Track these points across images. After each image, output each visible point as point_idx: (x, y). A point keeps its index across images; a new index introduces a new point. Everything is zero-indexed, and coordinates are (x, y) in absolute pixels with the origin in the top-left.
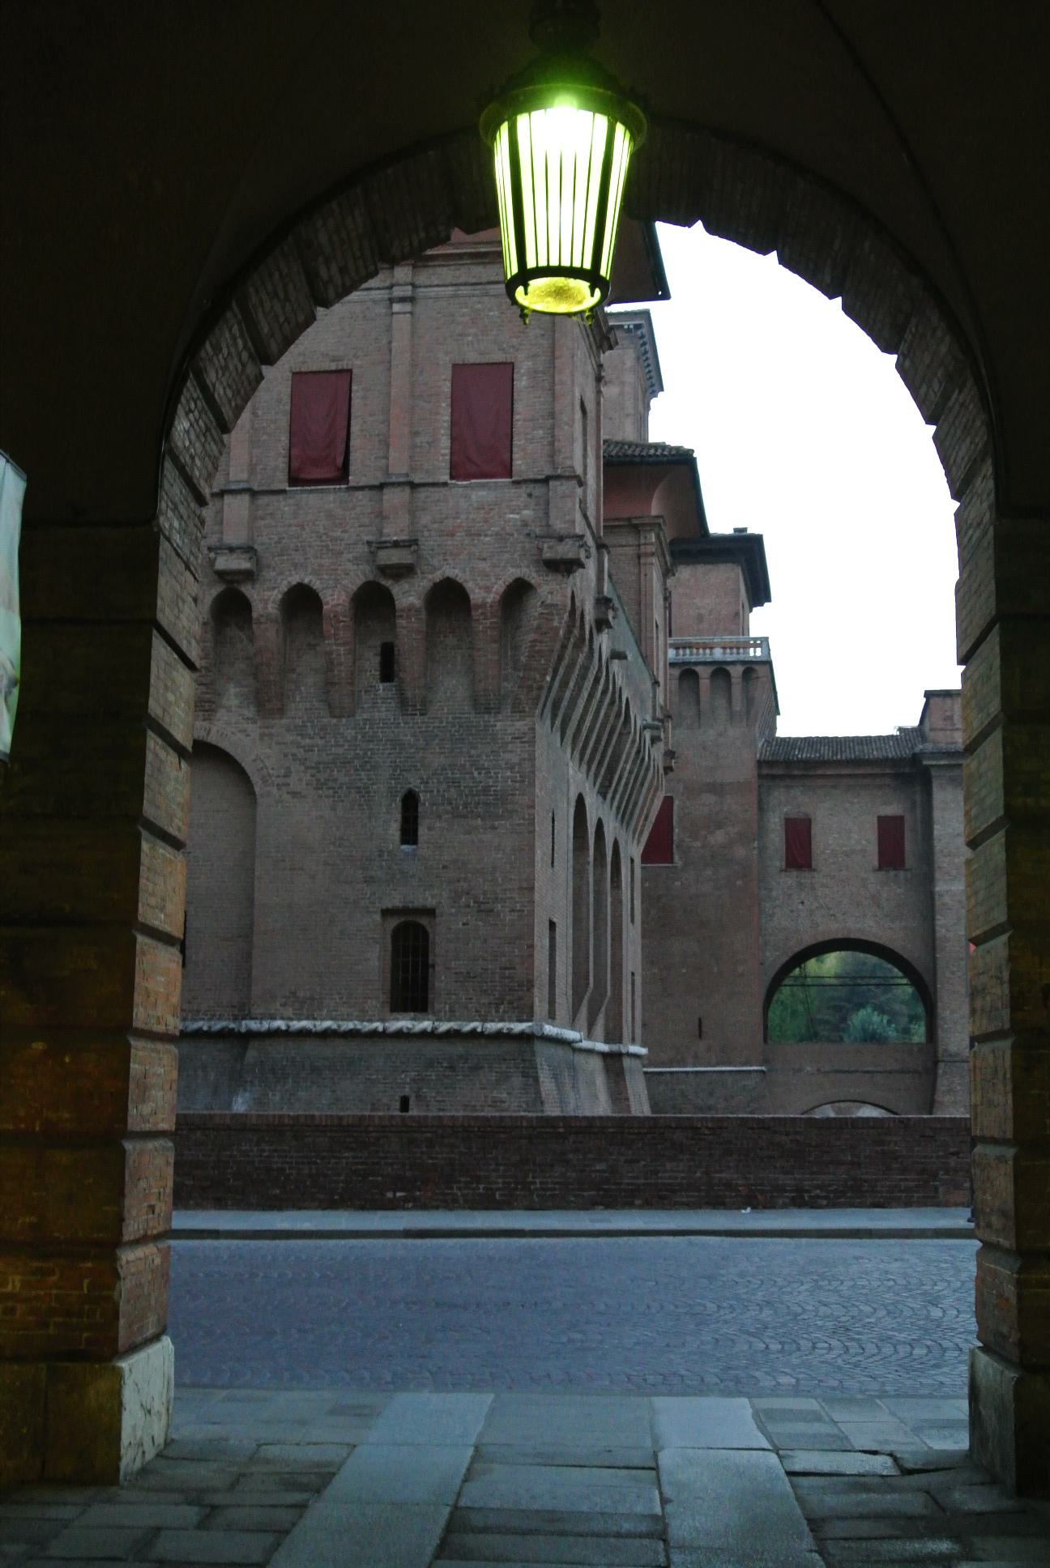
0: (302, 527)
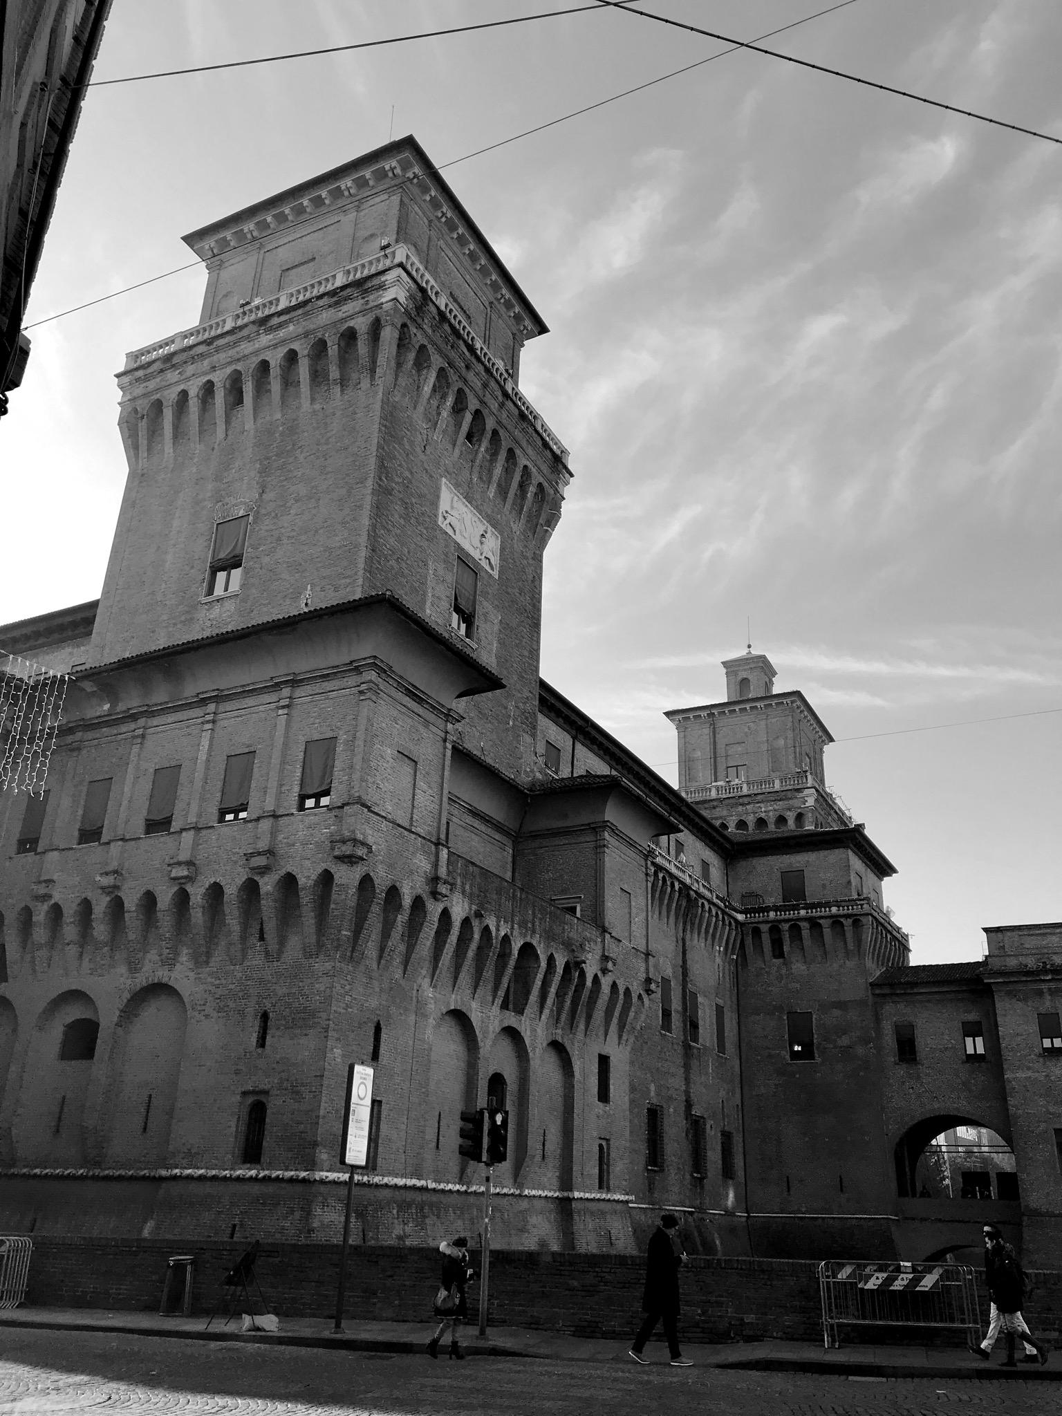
0: (219, 847)
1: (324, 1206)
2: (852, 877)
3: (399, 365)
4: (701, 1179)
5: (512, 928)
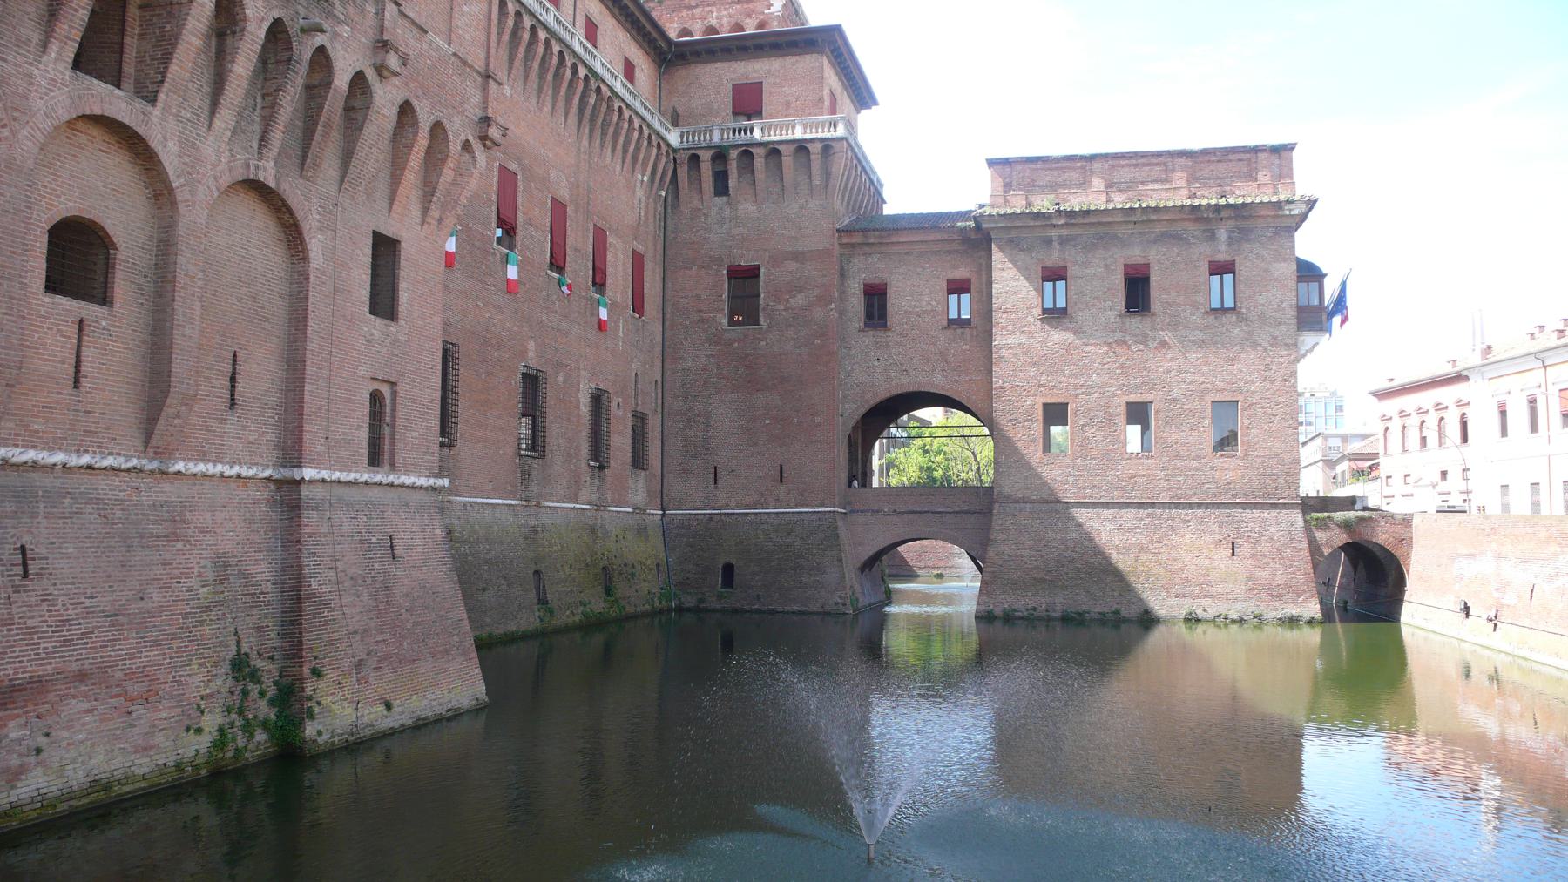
2: (825, 93)
4: (601, 468)
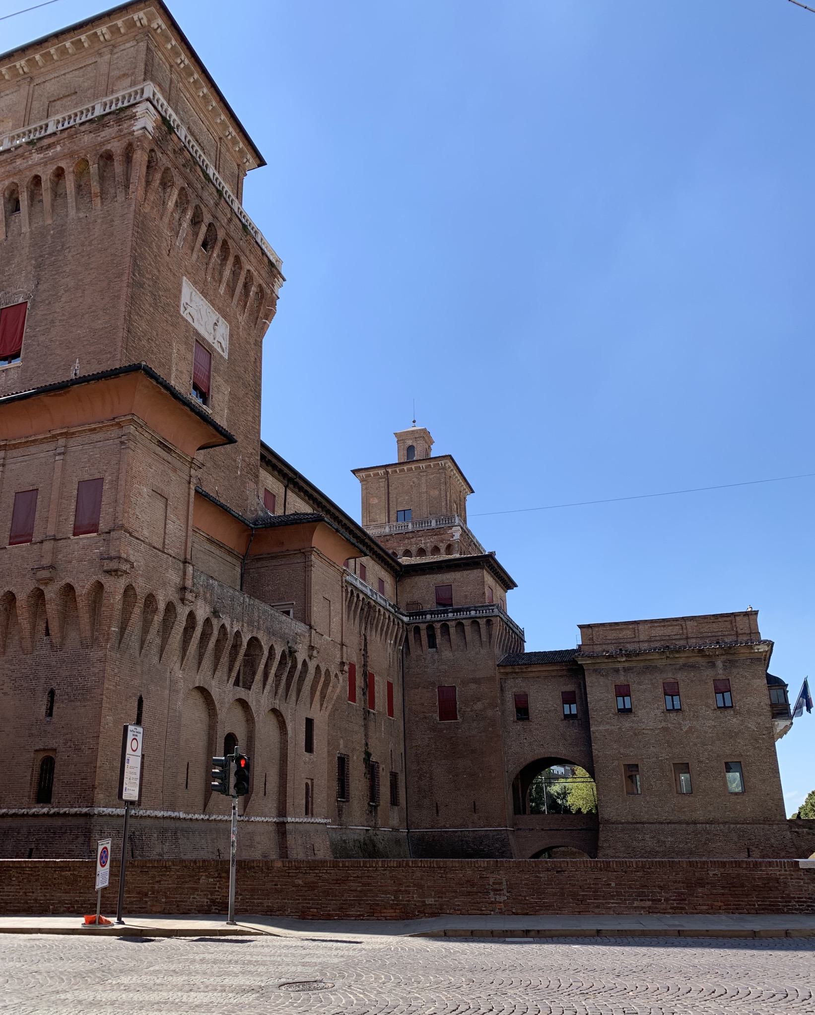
1: (101, 833)
2: (486, 590)
3: (148, 183)
5: (243, 626)
